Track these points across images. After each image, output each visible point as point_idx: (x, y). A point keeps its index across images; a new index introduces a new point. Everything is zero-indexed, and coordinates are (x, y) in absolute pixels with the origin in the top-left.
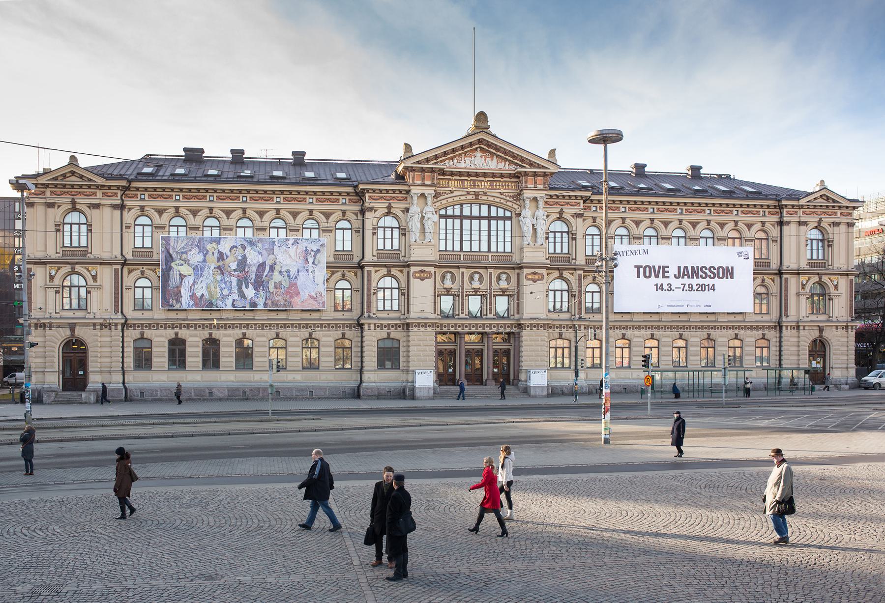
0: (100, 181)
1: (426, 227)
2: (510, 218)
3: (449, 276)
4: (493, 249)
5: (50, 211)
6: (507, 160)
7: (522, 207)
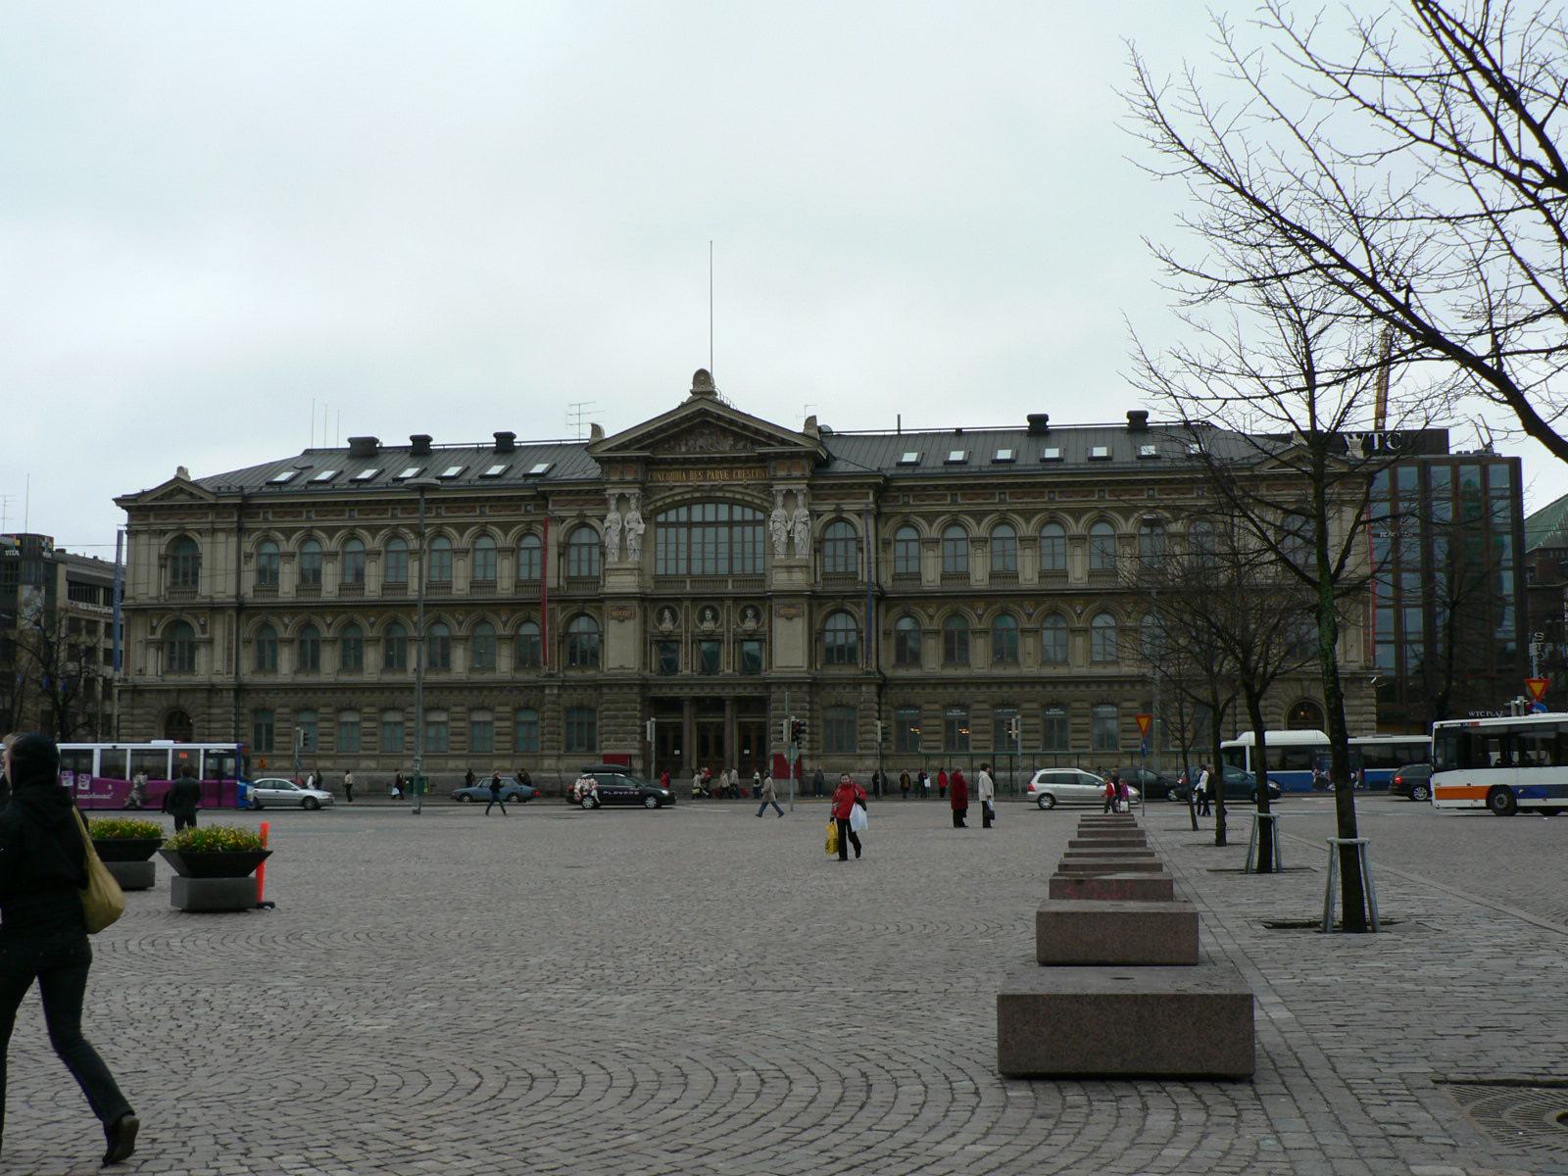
0: (212, 500)
1: (628, 542)
2: (762, 523)
3: (667, 613)
4: (737, 569)
5: (154, 541)
6: (747, 437)
7: (773, 504)
